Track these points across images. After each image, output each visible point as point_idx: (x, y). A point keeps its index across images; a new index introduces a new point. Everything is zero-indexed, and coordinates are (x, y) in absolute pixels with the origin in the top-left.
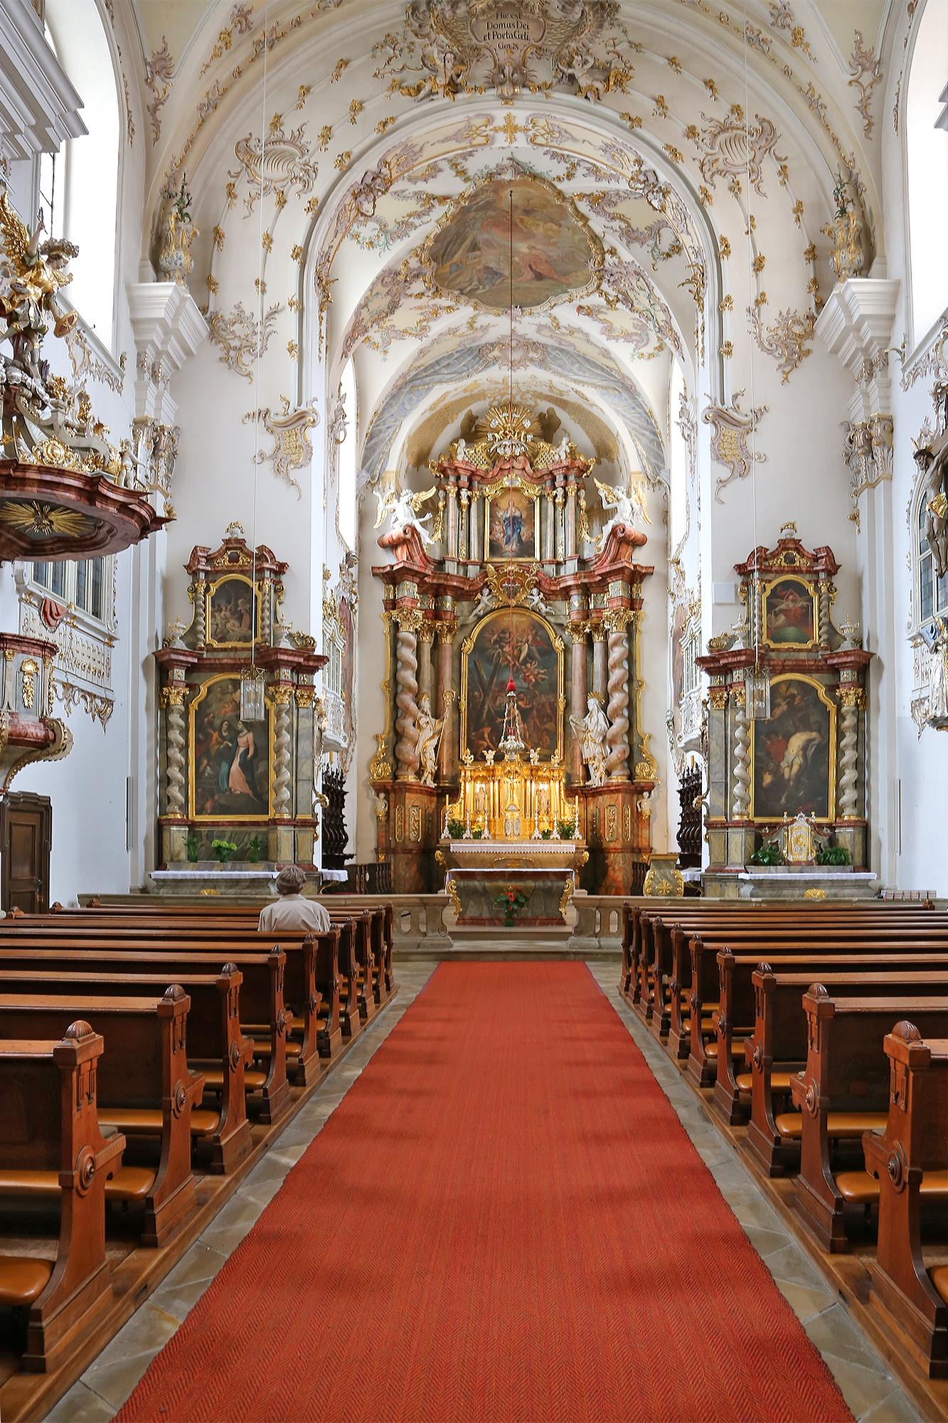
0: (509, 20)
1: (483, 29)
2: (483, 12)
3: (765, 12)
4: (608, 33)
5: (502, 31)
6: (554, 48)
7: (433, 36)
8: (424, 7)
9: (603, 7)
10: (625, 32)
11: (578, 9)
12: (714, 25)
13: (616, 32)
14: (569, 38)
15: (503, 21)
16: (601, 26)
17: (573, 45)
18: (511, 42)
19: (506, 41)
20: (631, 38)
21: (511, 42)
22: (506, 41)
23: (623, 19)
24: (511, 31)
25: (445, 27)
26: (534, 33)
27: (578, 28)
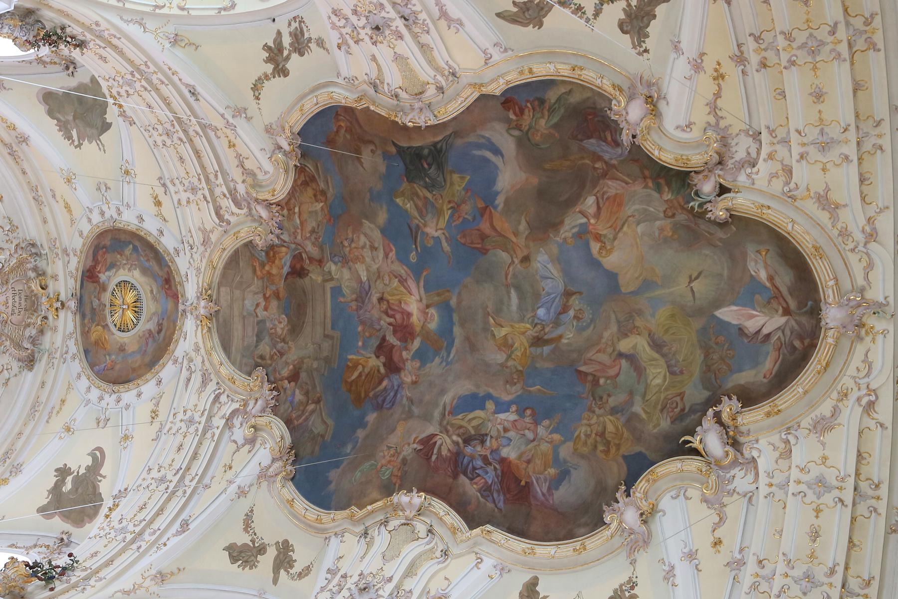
0: (23, 303)
1: (19, 287)
2: (29, 288)
3: (20, 461)
4: (15, 365)
5: (17, 299)
6: (6, 331)
7: (16, 256)
8: (33, 250)
9: (32, 361)
10: (16, 375)
11: (29, 346)
12: (17, 430)
13: (16, 369)
14: (12, 340)
15: (23, 300)
16: (19, 360)
17: (8, 343)
18: (10, 304)
19: (10, 301)
20: (12, 380)
21: (10, 304)
22: (10, 301)
23: (24, 373)
24: (17, 305)
25: (21, 263)
26: (15, 318)
27: (18, 346)
